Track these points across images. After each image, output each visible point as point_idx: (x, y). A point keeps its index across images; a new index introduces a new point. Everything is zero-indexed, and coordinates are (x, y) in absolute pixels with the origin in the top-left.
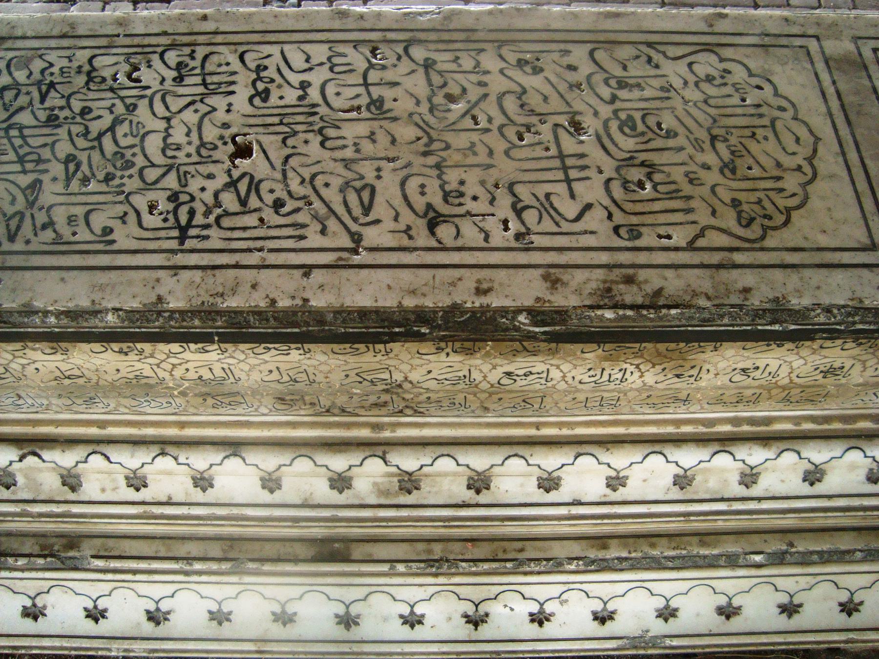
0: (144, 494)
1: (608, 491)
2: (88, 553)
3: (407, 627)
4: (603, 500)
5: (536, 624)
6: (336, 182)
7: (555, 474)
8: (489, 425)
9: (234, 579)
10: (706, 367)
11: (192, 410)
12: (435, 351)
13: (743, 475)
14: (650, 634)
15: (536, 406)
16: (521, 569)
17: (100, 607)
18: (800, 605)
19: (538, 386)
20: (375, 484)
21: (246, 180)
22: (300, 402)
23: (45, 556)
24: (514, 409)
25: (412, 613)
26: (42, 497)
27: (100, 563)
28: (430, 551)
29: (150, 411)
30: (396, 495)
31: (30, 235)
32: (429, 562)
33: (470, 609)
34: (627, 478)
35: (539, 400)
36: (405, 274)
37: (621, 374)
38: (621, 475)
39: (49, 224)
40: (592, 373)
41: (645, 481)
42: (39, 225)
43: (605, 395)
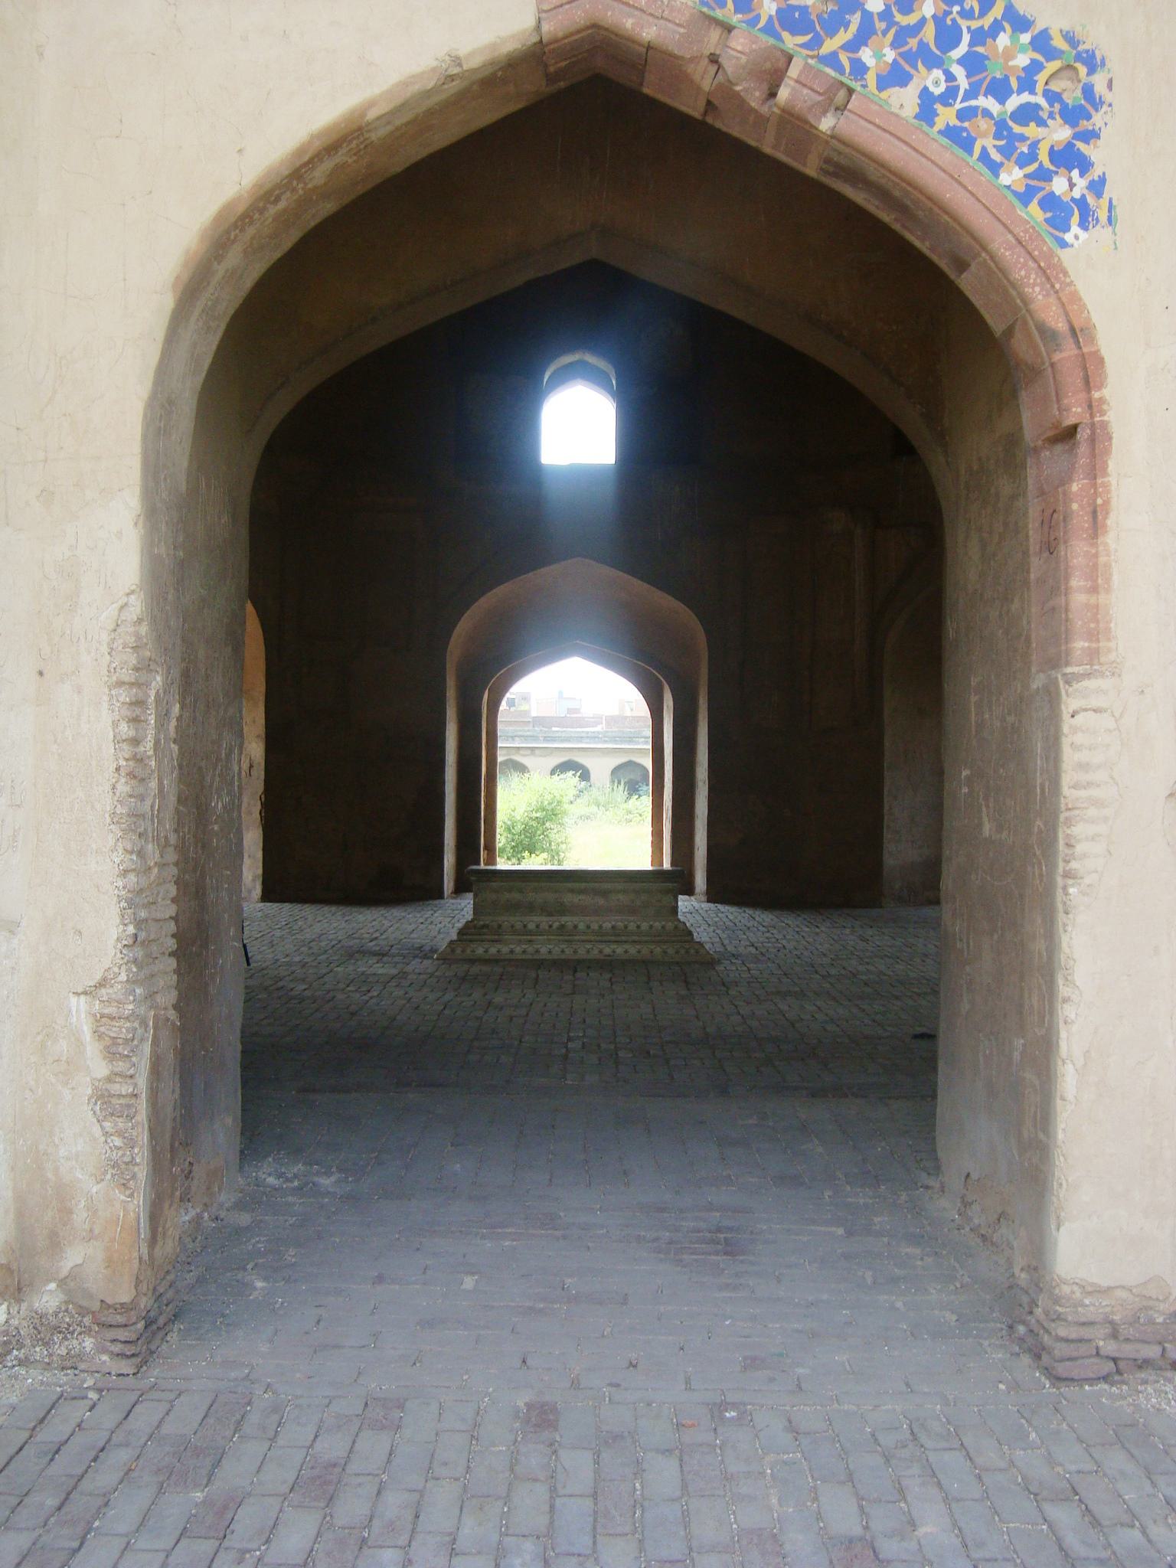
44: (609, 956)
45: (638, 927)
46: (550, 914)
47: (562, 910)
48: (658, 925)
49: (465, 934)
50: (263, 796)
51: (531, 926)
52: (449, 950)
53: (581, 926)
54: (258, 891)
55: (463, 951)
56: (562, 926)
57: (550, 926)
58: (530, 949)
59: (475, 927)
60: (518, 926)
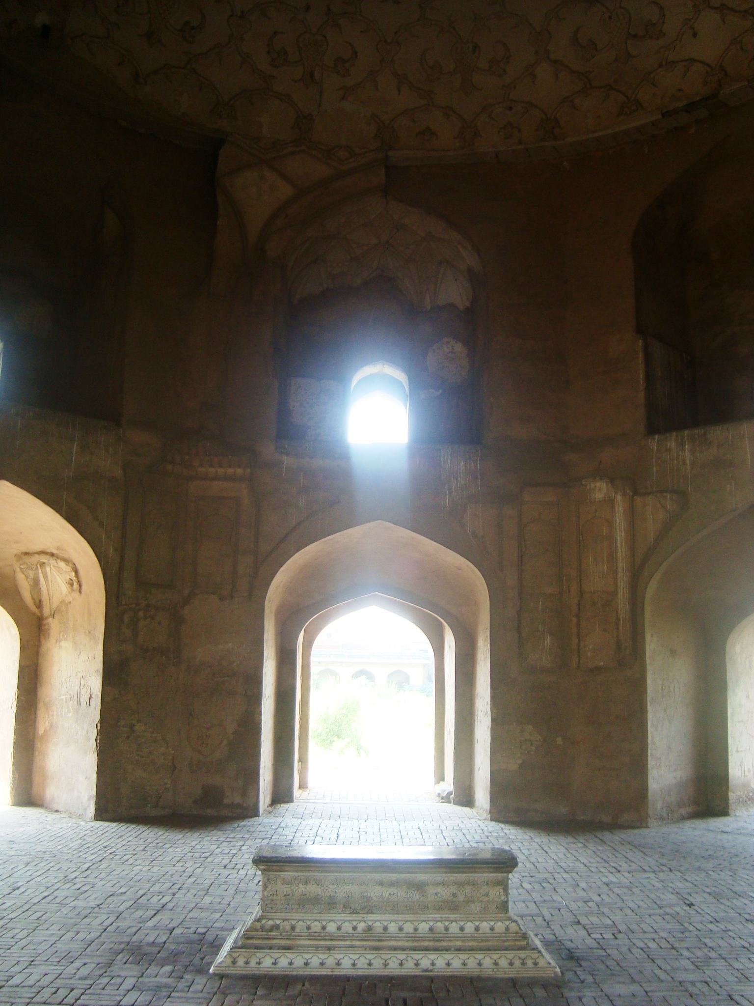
9: (328, 952)
19: (396, 900)
29: (316, 911)
44: (426, 970)
45: (462, 929)
46: (355, 912)
47: (368, 907)
48: (485, 926)
49: (252, 938)
50: (99, 725)
51: (332, 928)
52: (229, 961)
53: (393, 928)
54: (91, 811)
55: (247, 963)
56: (369, 929)
57: (355, 928)
58: (330, 962)
59: (262, 928)
60: (316, 927)
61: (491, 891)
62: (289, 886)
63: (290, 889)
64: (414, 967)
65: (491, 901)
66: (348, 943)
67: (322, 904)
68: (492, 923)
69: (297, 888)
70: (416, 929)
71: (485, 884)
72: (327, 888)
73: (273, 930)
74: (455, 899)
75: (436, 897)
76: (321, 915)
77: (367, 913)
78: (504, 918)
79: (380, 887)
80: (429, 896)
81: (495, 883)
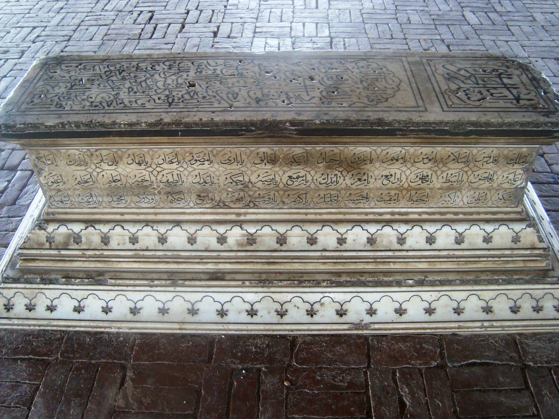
0: (137, 246)
1: (338, 245)
2: (108, 277)
3: (250, 316)
4: (336, 249)
5: (310, 316)
6: (224, 92)
7: (314, 236)
8: (285, 213)
9: (172, 289)
10: (370, 174)
11: (162, 205)
12: (260, 162)
13: (398, 239)
14: (364, 322)
15: (304, 200)
16: (301, 285)
17: (109, 306)
18: (435, 309)
20: (237, 240)
21: (193, 92)
22: (206, 198)
23: (88, 279)
24: (295, 203)
25: (252, 309)
26: (91, 248)
27: (113, 281)
28: (260, 277)
29: (144, 205)
30: (246, 246)
31: (115, 105)
32: (260, 281)
33: (278, 307)
34: (346, 238)
35: (304, 195)
36: (247, 113)
37: (335, 178)
38: (344, 237)
39: (123, 103)
40: (323, 177)
41: (354, 240)
42: (118, 103)
43: (332, 192)
44: (358, 326)
45: (431, 240)
55: (30, 308)
56: (251, 240)
57: (222, 240)
59: (50, 240)
61: (499, 173)
62: (83, 168)
63: (85, 173)
64: (337, 319)
65: (494, 189)
66: (211, 267)
67: (155, 194)
68: (489, 228)
69: (98, 170)
70: (341, 241)
71: (491, 160)
72: (159, 169)
73: (68, 245)
74: (423, 185)
75: (385, 182)
76: (157, 211)
77: (247, 206)
78: (512, 216)
79: (269, 166)
80: (372, 180)
81: (512, 160)
